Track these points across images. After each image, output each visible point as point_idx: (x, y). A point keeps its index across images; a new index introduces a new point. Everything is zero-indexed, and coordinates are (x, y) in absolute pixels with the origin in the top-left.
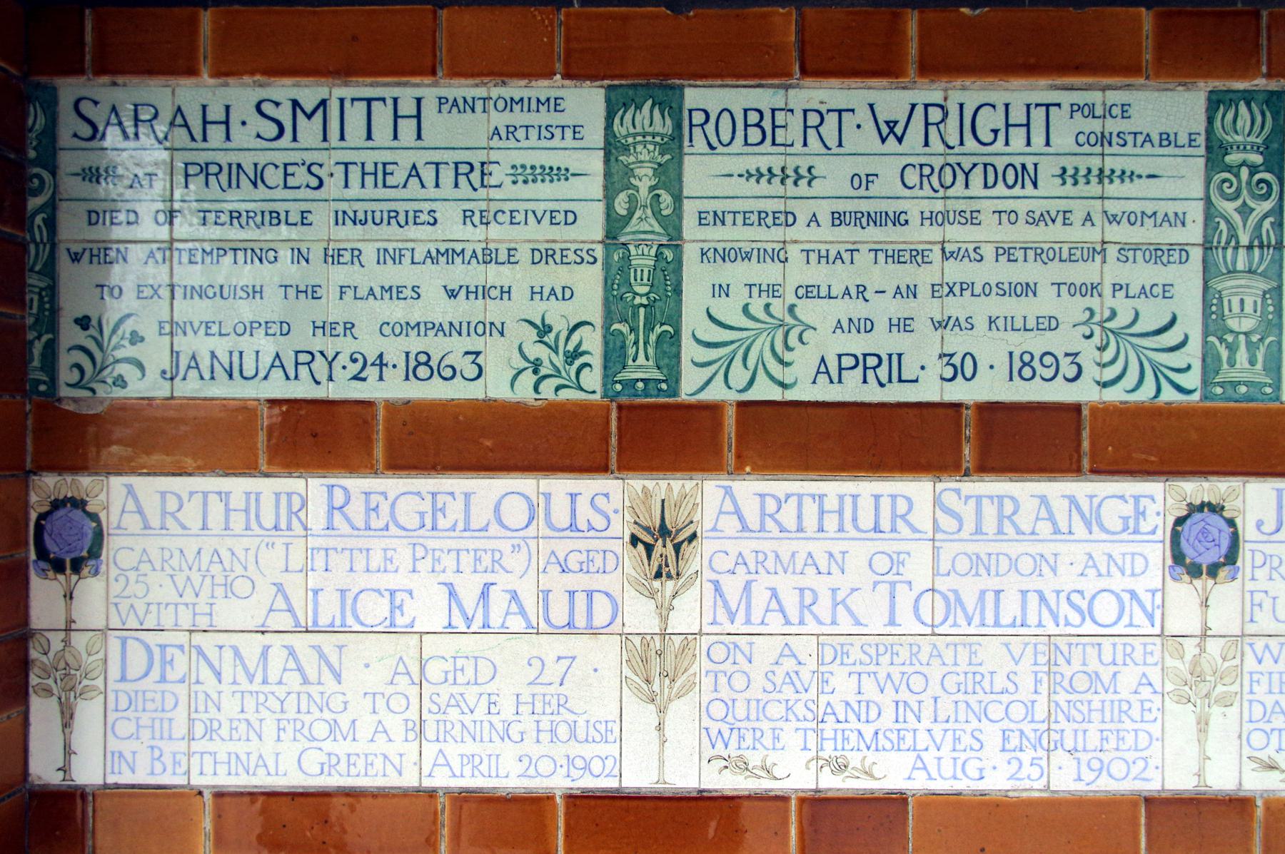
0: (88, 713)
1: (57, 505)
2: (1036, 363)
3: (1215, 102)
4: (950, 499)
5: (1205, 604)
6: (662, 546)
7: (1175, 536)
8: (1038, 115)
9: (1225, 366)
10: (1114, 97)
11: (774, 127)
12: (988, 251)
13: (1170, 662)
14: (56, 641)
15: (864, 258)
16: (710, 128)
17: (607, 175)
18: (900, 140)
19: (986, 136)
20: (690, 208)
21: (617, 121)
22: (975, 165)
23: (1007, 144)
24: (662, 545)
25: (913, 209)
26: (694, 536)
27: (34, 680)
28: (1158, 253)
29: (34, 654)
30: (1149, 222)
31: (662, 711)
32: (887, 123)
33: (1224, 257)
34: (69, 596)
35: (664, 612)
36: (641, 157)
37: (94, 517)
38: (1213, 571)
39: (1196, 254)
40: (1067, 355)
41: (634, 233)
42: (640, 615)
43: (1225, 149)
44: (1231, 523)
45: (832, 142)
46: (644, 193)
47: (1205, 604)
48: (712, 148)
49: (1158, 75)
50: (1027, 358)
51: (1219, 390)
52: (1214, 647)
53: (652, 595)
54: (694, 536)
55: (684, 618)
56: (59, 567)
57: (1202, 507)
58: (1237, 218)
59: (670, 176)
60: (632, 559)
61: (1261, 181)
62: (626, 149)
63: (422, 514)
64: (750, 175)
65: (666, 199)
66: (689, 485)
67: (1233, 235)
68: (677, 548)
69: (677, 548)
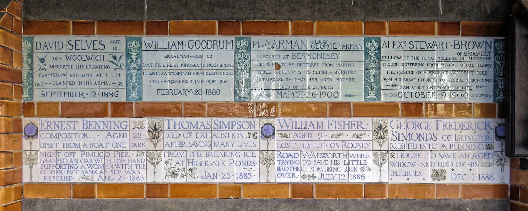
4: (216, 122)
6: (155, 132)
7: (262, 130)
13: (261, 156)
24: (155, 132)
26: (161, 130)
27: (24, 161)
29: (24, 156)
31: (155, 166)
34: (31, 143)
37: (36, 127)
42: (151, 146)
44: (273, 127)
52: (270, 152)
53: (153, 142)
54: (161, 130)
55: (160, 146)
56: (29, 137)
63: (126, 126)
68: (158, 132)
69: (158, 132)
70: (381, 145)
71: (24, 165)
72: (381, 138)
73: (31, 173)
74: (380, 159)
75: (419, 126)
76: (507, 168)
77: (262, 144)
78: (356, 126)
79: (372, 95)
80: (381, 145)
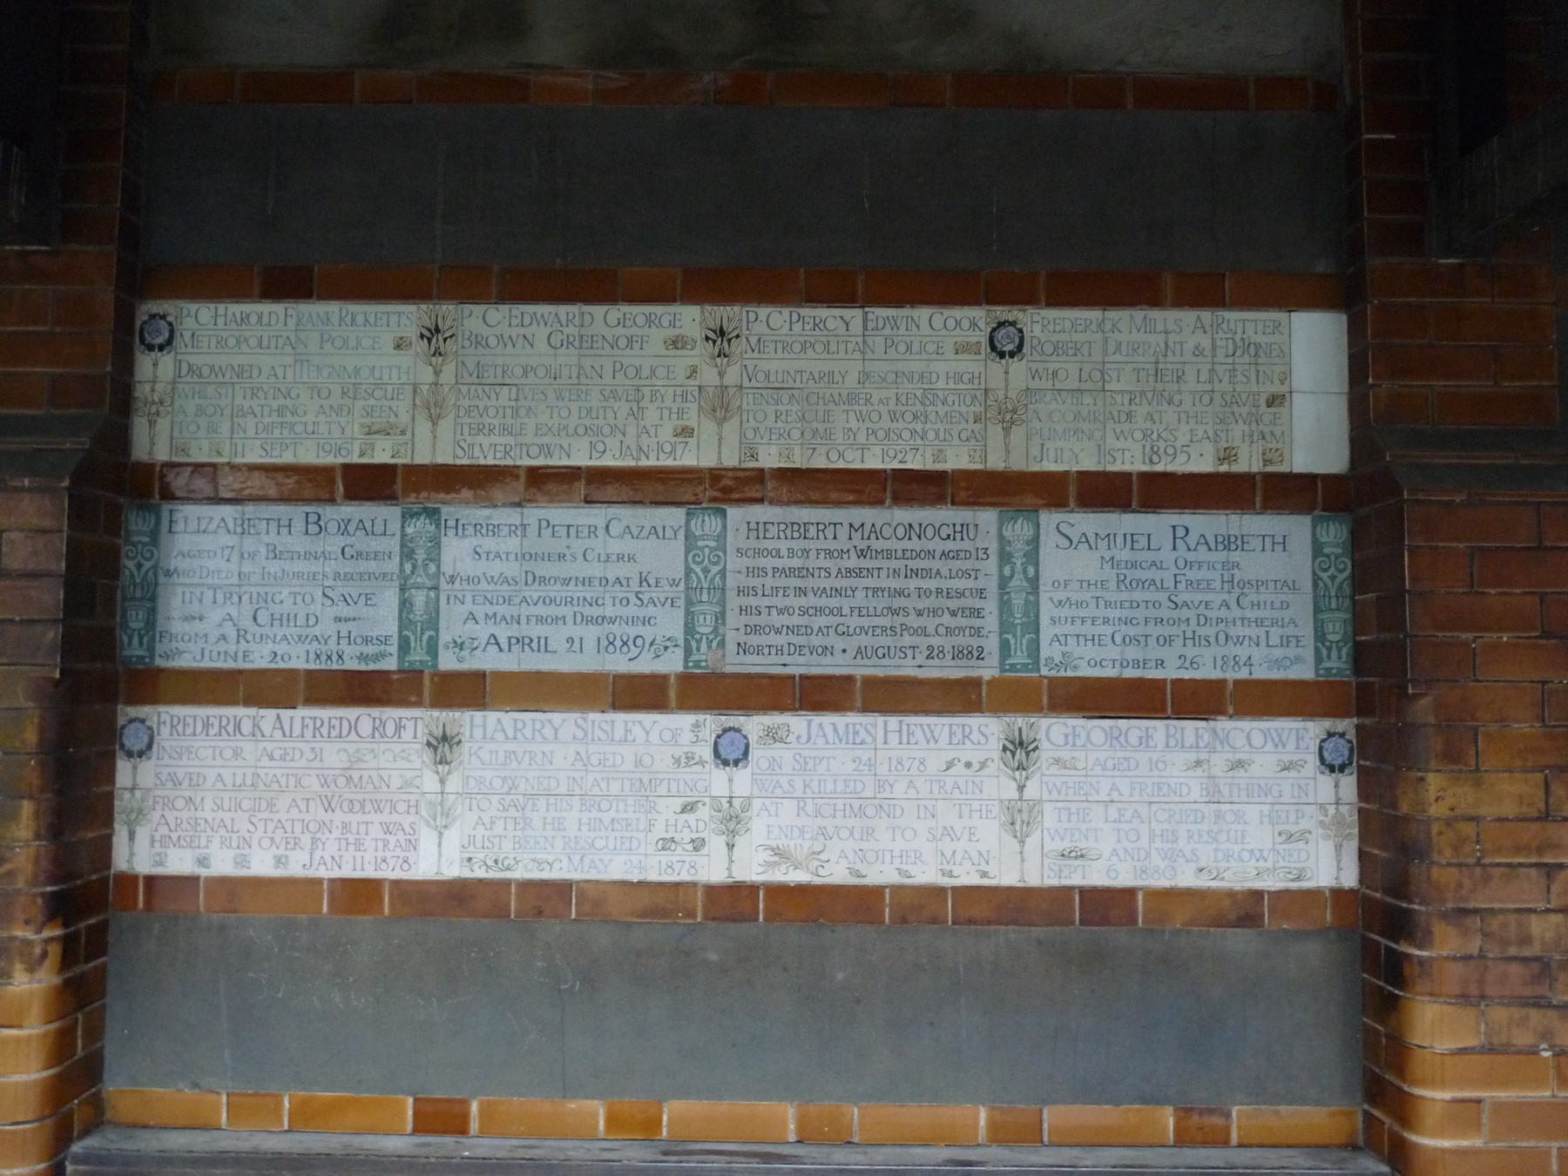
0: (142, 834)
1: (131, 721)
5: (730, 780)
7: (716, 743)
14: (127, 795)
24: (442, 745)
31: (441, 834)
34: (135, 768)
35: (442, 782)
38: (736, 763)
42: (430, 782)
44: (745, 737)
47: (730, 780)
52: (736, 803)
55: (454, 784)
56: (130, 754)
57: (730, 729)
60: (428, 756)
66: (457, 714)
70: (1021, 788)
71: (117, 826)
72: (1021, 767)
73: (131, 848)
74: (1019, 819)
75: (1122, 739)
76: (1352, 847)
77: (719, 781)
78: (959, 736)
79: (1019, 657)
80: (1021, 788)
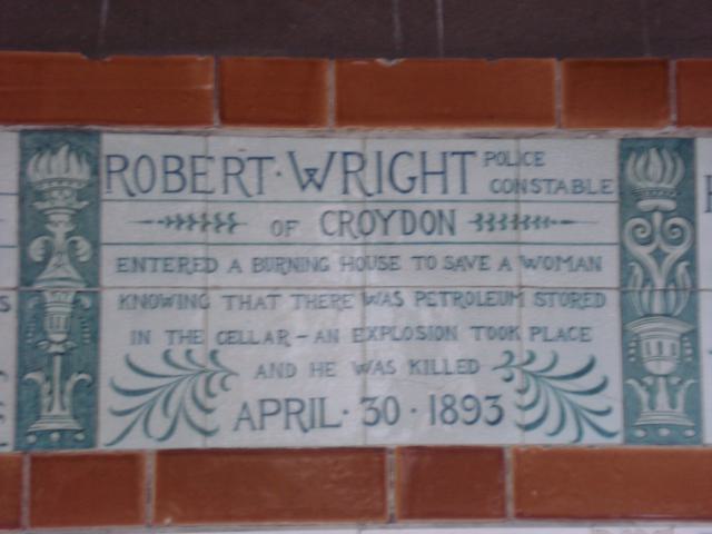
2: (457, 407)
3: (627, 150)
8: (454, 162)
9: (646, 409)
10: (528, 145)
11: (195, 174)
12: (407, 295)
15: (286, 303)
16: (128, 174)
17: (22, 220)
18: (319, 187)
19: (403, 183)
20: (109, 255)
21: (32, 163)
22: (393, 212)
23: (424, 192)
25: (334, 256)
28: (573, 298)
30: (564, 267)
32: (307, 170)
33: (641, 300)
36: (57, 204)
39: (613, 298)
40: (488, 398)
41: (52, 279)
43: (638, 195)
45: (253, 189)
46: (59, 240)
48: (132, 195)
49: (569, 125)
50: (448, 401)
51: (640, 433)
58: (651, 262)
59: (87, 222)
61: (674, 226)
62: (40, 196)
64: (181, 222)
65: (84, 246)
67: (647, 280)
